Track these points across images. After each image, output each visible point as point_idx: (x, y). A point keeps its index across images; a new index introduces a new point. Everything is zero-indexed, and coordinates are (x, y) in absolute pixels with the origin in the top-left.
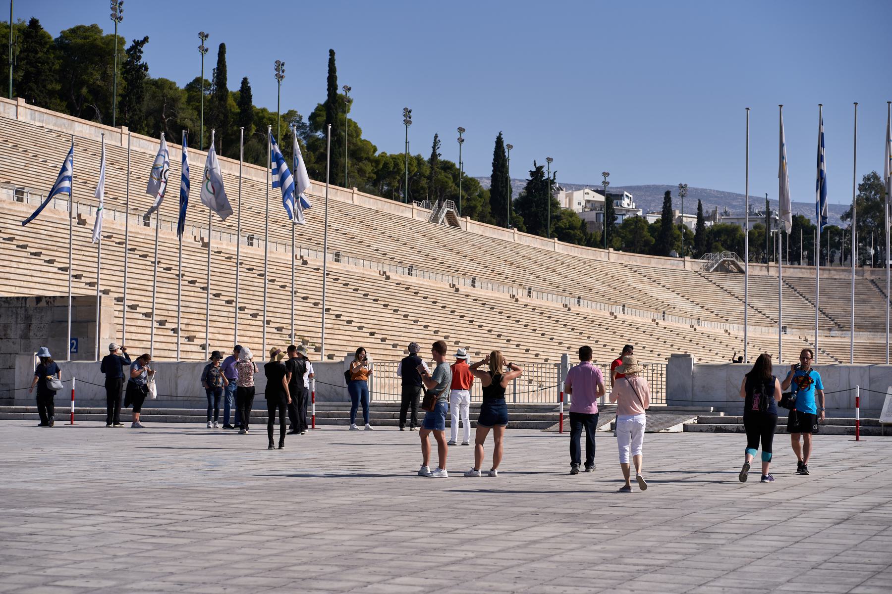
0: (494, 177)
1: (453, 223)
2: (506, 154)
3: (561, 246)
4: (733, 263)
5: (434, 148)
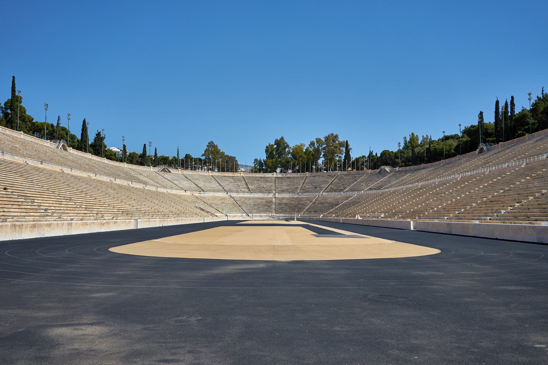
0: (82, 135)
1: (65, 149)
2: (87, 126)
3: (107, 161)
4: (167, 169)
5: (58, 121)
